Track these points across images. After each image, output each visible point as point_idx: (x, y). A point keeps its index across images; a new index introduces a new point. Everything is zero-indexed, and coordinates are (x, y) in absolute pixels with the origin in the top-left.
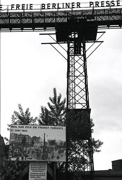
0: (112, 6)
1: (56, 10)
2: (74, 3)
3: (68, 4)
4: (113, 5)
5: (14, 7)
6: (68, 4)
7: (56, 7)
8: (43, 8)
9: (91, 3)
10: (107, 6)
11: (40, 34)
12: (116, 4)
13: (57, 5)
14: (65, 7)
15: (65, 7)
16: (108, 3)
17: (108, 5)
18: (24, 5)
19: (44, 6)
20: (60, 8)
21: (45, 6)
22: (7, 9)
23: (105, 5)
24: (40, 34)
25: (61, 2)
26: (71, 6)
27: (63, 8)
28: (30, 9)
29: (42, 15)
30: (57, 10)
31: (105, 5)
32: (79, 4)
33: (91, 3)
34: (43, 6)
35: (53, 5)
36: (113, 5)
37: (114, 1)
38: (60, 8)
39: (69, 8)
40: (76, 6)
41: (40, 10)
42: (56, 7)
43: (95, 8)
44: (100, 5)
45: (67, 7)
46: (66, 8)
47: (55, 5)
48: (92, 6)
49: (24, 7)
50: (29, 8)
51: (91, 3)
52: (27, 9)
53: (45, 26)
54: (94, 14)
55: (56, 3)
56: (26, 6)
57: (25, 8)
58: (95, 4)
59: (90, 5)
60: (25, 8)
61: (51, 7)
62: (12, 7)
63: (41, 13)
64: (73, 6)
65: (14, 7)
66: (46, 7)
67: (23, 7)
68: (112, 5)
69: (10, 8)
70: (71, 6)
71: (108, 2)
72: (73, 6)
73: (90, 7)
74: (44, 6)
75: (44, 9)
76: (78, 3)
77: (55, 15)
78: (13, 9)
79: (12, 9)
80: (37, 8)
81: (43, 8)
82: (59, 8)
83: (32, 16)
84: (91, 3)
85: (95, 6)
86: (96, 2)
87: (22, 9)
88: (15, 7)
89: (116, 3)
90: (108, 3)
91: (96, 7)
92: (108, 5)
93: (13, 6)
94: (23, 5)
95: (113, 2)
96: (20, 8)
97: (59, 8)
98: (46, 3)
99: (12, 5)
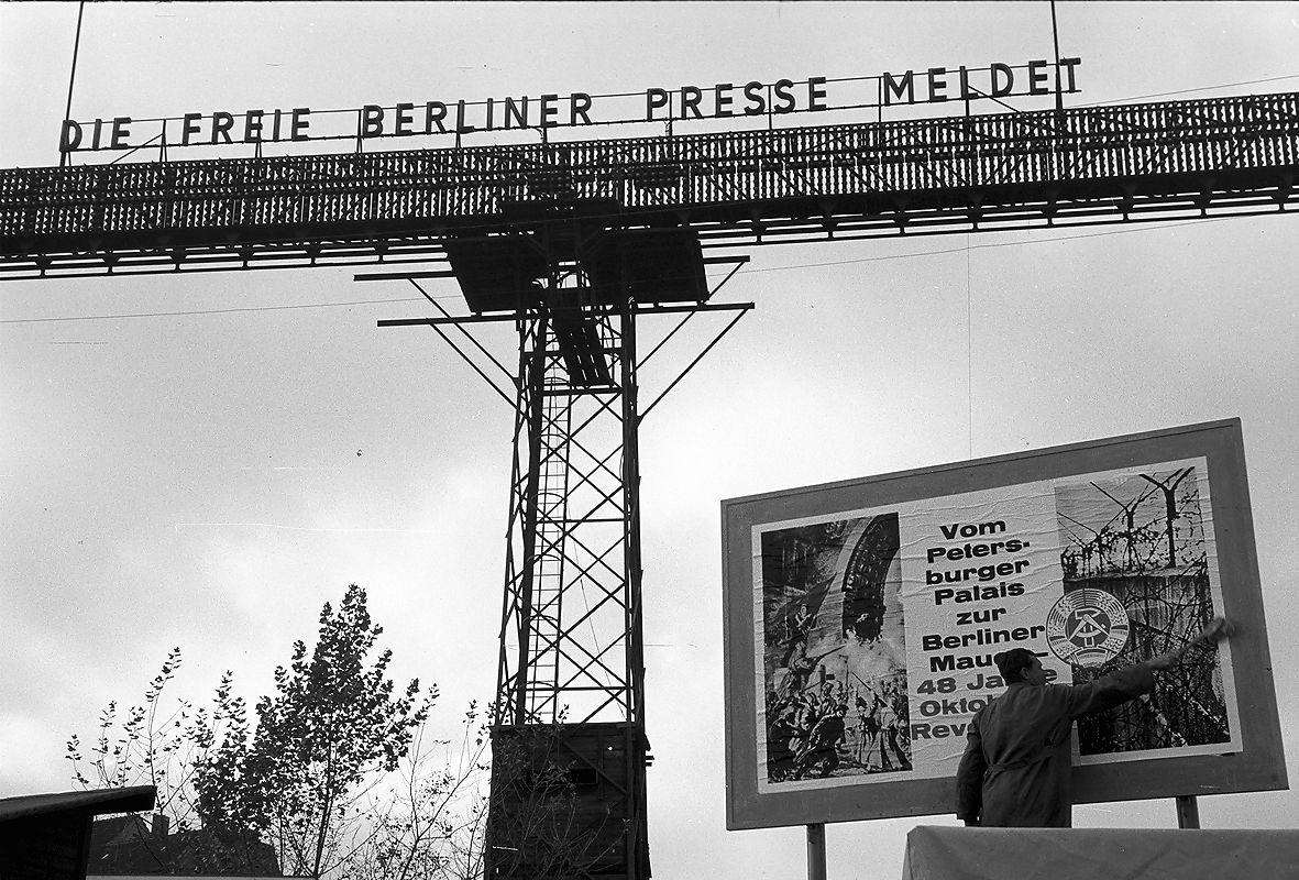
0: (779, 110)
1: (448, 142)
2: (729, 87)
3: (519, 106)
4: (785, 104)
5: (197, 130)
6: (519, 106)
7: (450, 122)
8: (372, 128)
9: (657, 98)
10: (749, 112)
11: (357, 278)
12: (802, 101)
13: (452, 112)
14: (499, 121)
15: (499, 121)
16: (754, 91)
17: (755, 105)
18: (260, 114)
19: (373, 121)
20: (471, 129)
21: (381, 117)
22: (159, 141)
23: (740, 102)
24: (357, 278)
25: (476, 93)
26: (534, 117)
27: (490, 128)
28: (115, 146)
29: (361, 171)
30: (354, 150)
31: (740, 102)
32: (581, 106)
33: (657, 98)
34: (370, 121)
35: (573, 104)
36: (785, 104)
37: (790, 84)
38: (471, 129)
39: (524, 126)
40: (564, 115)
41: (349, 147)
42: (450, 122)
43: (680, 129)
44: (707, 105)
45: (514, 122)
46: (507, 127)
47: (443, 114)
48: (657, 113)
49: (259, 127)
50: (286, 132)
51: (656, 98)
52: (276, 139)
53: (380, 236)
54: (664, 164)
55: (449, 98)
56: (268, 122)
57: (267, 133)
58: (677, 99)
59: (652, 105)
60: (267, 133)
61: (419, 123)
62: (188, 130)
63: (358, 159)
64: (550, 118)
65: (197, 130)
66: (389, 124)
67: (250, 126)
68: (777, 107)
69: (175, 133)
70: (534, 117)
71: (759, 86)
72: (550, 118)
73: (650, 119)
74: (373, 121)
75: (378, 134)
76: (575, 97)
77: (435, 170)
78: (193, 138)
79: (185, 143)
80: (332, 136)
81: (372, 128)
82: (462, 129)
83: (305, 176)
84: (656, 98)
85: (677, 113)
86: (685, 90)
87: (248, 140)
88: (206, 126)
89: (801, 95)
90: (754, 91)
91: (684, 117)
92: (755, 105)
93: (193, 123)
94: (250, 114)
95: (784, 89)
96: (238, 131)
97: (462, 129)
98: (388, 102)
99: (189, 117)
